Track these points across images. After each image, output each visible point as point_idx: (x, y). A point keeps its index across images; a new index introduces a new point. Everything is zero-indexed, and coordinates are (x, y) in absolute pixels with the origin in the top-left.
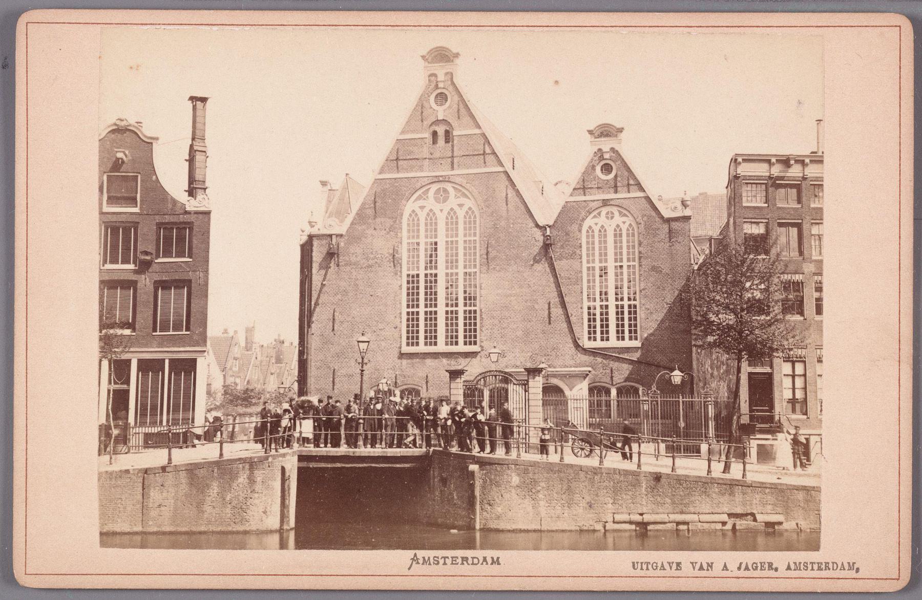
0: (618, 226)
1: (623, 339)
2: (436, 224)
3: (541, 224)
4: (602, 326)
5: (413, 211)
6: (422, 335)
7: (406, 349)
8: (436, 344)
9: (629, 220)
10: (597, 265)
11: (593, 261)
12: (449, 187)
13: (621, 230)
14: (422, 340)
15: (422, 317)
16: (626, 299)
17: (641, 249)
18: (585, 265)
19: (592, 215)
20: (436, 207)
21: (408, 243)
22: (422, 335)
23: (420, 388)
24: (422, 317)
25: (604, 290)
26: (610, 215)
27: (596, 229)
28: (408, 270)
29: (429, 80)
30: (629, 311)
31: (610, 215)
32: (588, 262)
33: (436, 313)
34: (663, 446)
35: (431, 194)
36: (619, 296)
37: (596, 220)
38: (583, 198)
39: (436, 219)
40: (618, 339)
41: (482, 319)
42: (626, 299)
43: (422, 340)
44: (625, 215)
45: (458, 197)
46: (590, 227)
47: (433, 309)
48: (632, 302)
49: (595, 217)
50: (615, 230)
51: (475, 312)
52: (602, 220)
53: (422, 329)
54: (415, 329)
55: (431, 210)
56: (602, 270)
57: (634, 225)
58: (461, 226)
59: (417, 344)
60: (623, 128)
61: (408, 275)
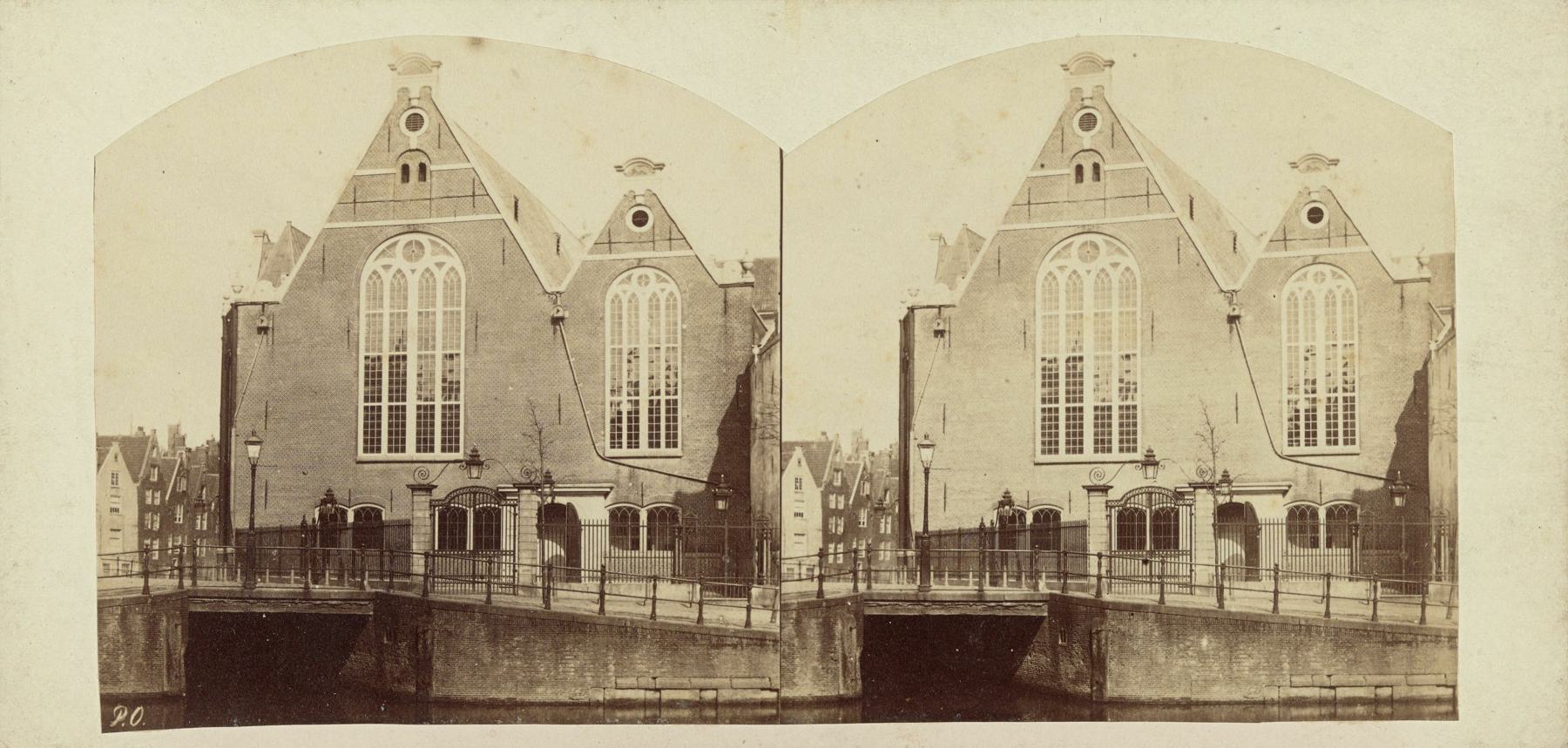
0: (1331, 291)
1: (1336, 443)
2: (1081, 290)
3: (1225, 290)
4: (1307, 426)
5: (1050, 273)
6: (1062, 439)
7: (1041, 458)
8: (1081, 451)
9: (1347, 283)
10: (1302, 345)
11: (1297, 339)
12: (1098, 239)
13: (1334, 297)
14: (1062, 446)
15: (1062, 415)
16: (1340, 390)
17: (1361, 322)
18: (1285, 345)
19: (1294, 277)
20: (1082, 269)
21: (1044, 317)
22: (1062, 439)
23: (1060, 510)
24: (1062, 415)
25: (1311, 378)
26: (1320, 277)
27: (1301, 295)
28: (1044, 351)
29: (1071, 97)
30: (1354, 410)
31: (1320, 277)
32: (1289, 340)
33: (1081, 409)
34: (1379, 584)
35: (1074, 250)
36: (1332, 387)
37: (1300, 284)
38: (1285, 254)
39: (1082, 283)
40: (1329, 442)
41: (1143, 417)
42: (1340, 390)
43: (1062, 446)
44: (1340, 277)
45: (1112, 254)
46: (1292, 294)
47: (1077, 405)
48: (1348, 394)
49: (1298, 279)
50: (1327, 297)
51: (1135, 407)
52: (1310, 284)
53: (1062, 431)
54: (1053, 431)
55: (1075, 272)
56: (1308, 351)
57: (1352, 288)
58: (1115, 293)
59: (1057, 451)
60: (1338, 161)
61: (1043, 359)
